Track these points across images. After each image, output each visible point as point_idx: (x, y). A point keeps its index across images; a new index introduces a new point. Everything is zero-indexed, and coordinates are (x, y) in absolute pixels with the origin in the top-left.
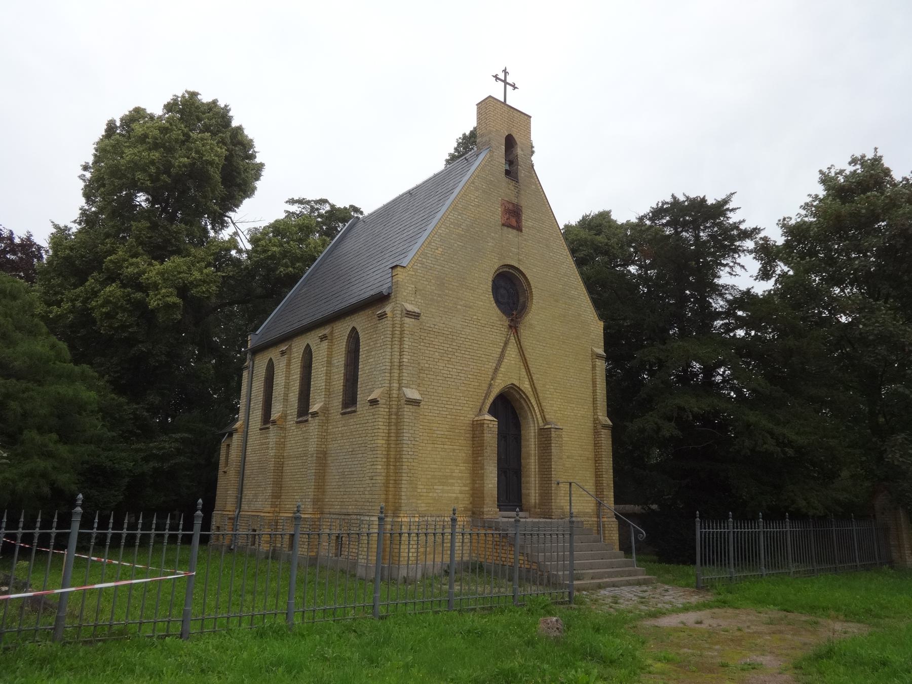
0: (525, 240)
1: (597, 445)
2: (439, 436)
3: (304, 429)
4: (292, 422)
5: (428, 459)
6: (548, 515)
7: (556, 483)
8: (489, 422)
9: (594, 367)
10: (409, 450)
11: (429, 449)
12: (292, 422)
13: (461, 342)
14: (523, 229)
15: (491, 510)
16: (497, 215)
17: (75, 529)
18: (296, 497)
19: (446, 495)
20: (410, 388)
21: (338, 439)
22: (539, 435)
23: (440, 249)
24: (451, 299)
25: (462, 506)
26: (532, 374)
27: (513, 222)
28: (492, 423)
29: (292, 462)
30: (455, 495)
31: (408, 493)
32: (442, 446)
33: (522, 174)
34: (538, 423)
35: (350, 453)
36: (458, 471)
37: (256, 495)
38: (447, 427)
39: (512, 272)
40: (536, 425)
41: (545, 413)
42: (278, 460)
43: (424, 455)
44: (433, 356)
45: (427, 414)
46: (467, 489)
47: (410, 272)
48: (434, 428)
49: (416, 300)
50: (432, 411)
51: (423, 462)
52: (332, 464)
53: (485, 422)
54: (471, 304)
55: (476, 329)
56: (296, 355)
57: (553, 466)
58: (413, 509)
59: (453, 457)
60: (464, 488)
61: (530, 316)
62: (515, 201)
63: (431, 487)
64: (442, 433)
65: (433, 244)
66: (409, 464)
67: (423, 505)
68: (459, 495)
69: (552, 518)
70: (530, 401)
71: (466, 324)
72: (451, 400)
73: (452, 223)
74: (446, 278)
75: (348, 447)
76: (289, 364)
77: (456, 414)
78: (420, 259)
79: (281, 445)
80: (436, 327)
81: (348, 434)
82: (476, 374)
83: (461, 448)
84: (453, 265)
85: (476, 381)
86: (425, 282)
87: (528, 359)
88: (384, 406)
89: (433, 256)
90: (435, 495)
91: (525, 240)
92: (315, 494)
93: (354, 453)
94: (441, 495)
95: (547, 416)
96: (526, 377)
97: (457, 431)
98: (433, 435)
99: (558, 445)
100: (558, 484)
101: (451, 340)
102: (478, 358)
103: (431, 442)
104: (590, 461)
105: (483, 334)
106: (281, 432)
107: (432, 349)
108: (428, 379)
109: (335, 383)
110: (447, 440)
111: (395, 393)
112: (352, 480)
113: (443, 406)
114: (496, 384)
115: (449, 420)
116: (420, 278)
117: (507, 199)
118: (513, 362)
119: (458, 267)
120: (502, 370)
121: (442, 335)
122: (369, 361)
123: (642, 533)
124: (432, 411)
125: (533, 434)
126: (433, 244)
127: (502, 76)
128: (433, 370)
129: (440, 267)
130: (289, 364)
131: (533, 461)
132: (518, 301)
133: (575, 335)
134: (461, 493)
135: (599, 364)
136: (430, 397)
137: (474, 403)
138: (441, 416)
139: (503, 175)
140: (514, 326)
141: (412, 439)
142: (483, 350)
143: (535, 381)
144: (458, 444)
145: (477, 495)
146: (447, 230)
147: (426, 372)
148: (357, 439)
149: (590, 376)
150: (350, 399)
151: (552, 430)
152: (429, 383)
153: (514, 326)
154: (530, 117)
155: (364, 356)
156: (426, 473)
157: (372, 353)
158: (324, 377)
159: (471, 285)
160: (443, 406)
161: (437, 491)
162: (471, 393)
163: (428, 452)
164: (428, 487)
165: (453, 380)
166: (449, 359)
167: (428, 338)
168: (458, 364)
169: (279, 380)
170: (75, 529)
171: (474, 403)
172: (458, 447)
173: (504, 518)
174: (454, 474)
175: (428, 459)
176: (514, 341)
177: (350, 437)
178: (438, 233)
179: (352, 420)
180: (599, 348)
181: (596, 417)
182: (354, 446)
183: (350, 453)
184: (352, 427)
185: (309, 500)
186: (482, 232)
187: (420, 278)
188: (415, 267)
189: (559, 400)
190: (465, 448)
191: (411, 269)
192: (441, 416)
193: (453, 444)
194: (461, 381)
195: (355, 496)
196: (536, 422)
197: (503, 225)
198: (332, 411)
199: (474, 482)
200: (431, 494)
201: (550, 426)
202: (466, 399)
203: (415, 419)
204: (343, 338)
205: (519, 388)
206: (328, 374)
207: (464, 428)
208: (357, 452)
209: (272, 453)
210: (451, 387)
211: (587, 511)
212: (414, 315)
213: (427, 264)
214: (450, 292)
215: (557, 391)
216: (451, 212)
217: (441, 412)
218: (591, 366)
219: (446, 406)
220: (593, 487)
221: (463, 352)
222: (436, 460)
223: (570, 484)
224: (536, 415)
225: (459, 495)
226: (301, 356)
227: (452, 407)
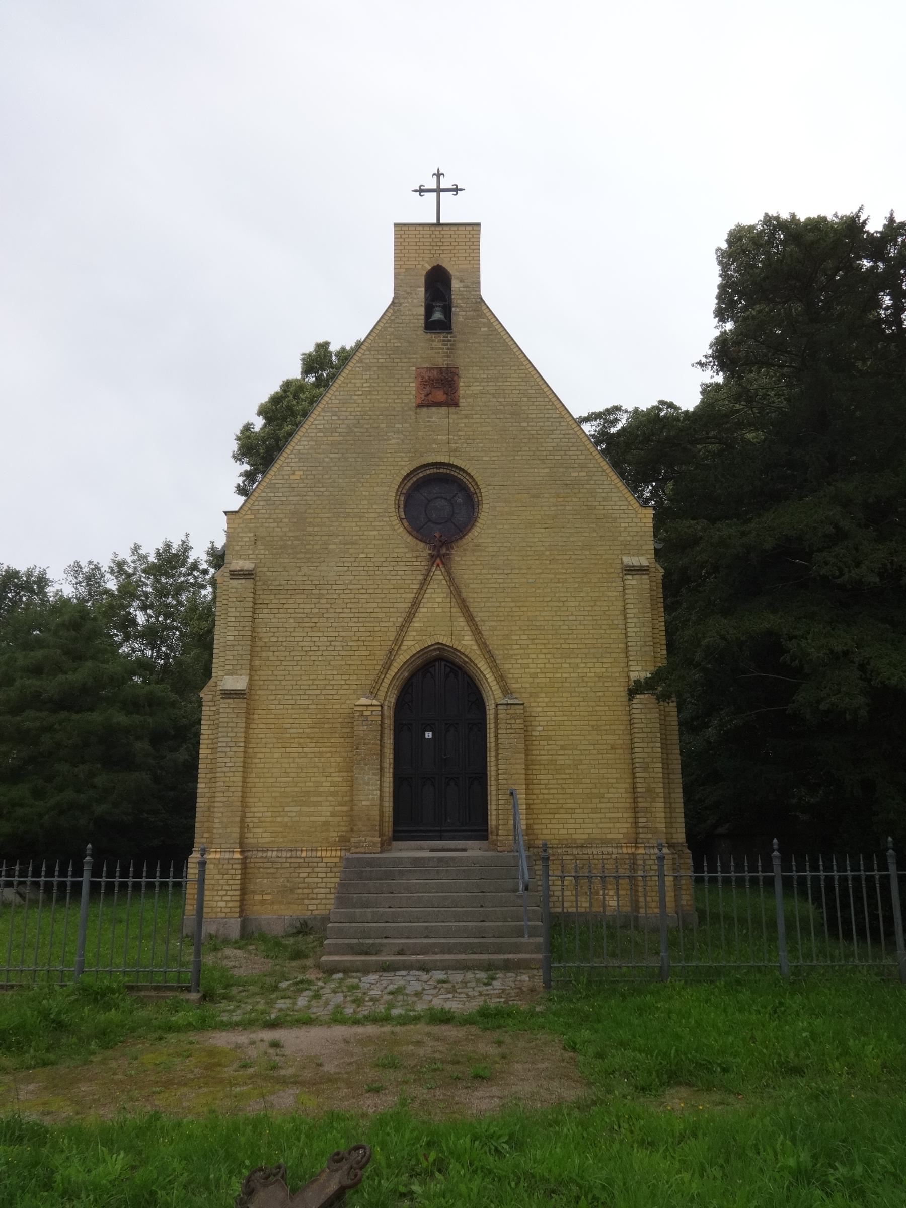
0: (466, 417)
2: (293, 736)
7: (509, 792)
8: (365, 708)
11: (276, 755)
13: (335, 596)
17: (86, 878)
19: (307, 819)
20: (236, 674)
24: (317, 538)
25: (335, 834)
27: (440, 396)
30: (323, 819)
31: (225, 820)
32: (300, 750)
33: (459, 316)
36: (329, 784)
38: (309, 721)
39: (445, 471)
44: (287, 625)
45: (273, 707)
48: (285, 726)
49: (257, 552)
50: (283, 702)
51: (267, 775)
54: (355, 538)
58: (232, 841)
59: (320, 765)
61: (475, 531)
63: (280, 809)
64: (301, 731)
67: (264, 835)
68: (330, 819)
73: (320, 430)
74: (308, 511)
77: (325, 702)
78: (264, 494)
80: (290, 583)
83: (334, 750)
84: (322, 490)
85: (364, 648)
86: (272, 525)
89: (285, 485)
90: (286, 820)
91: (466, 417)
94: (298, 819)
96: (467, 628)
98: (284, 736)
101: (317, 596)
102: (368, 615)
103: (280, 745)
105: (378, 577)
107: (283, 615)
108: (275, 658)
110: (308, 740)
113: (302, 692)
115: (313, 711)
117: (427, 365)
118: (440, 610)
120: (416, 624)
121: (300, 592)
124: (283, 702)
126: (285, 468)
128: (284, 644)
129: (298, 498)
133: (580, 543)
134: (333, 814)
135: (634, 582)
136: (278, 683)
138: (298, 707)
141: (232, 744)
144: (330, 745)
146: (311, 443)
147: (272, 649)
152: (278, 663)
154: (479, 225)
156: (271, 789)
160: (302, 692)
161: (289, 814)
162: (353, 668)
163: (275, 760)
164: (275, 810)
166: (313, 625)
167: (277, 601)
170: (86, 878)
172: (328, 750)
174: (321, 789)
176: (442, 577)
178: (295, 452)
188: (257, 507)
190: (342, 750)
191: (249, 512)
192: (298, 707)
193: (318, 745)
194: (336, 653)
197: (419, 406)
200: (279, 820)
202: (344, 677)
203: (237, 716)
205: (452, 648)
207: (340, 720)
210: (317, 663)
211: (609, 836)
212: (244, 575)
213: (276, 499)
215: (536, 641)
217: (298, 702)
219: (308, 692)
221: (341, 610)
222: (288, 770)
225: (330, 819)
227: (318, 692)
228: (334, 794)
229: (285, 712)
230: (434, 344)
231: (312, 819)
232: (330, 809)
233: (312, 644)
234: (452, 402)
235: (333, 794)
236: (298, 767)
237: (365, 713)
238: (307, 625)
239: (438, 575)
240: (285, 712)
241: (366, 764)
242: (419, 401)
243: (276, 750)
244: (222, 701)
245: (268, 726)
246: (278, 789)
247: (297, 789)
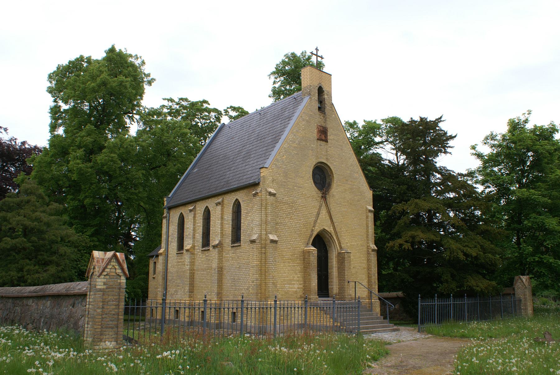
0: (330, 147)
1: (368, 260)
2: (287, 259)
3: (207, 254)
4: (199, 250)
5: (282, 271)
6: (342, 298)
8: (313, 251)
9: (367, 217)
10: (273, 267)
11: (282, 266)
12: (199, 250)
13: (297, 207)
14: (328, 141)
15: (314, 297)
18: (204, 292)
21: (230, 260)
22: (338, 256)
23: (285, 156)
26: (334, 223)
28: (315, 251)
29: (200, 273)
30: (295, 290)
31: (273, 289)
32: (288, 264)
33: (328, 108)
34: (337, 250)
35: (238, 268)
36: (296, 277)
37: (176, 291)
40: (336, 251)
41: (341, 244)
42: (191, 271)
43: (279, 269)
45: (280, 247)
46: (301, 286)
47: (270, 170)
50: (283, 245)
52: (226, 274)
53: (311, 250)
55: (304, 200)
56: (199, 212)
57: (346, 273)
59: (294, 270)
60: (300, 286)
62: (324, 125)
63: (283, 286)
64: (288, 257)
65: (281, 153)
66: (273, 274)
69: (345, 301)
70: (333, 238)
71: (299, 197)
72: (292, 239)
75: (236, 265)
80: (284, 200)
81: (236, 258)
82: (305, 224)
83: (298, 265)
85: (305, 228)
87: (332, 215)
88: (259, 244)
92: (218, 290)
93: (240, 268)
95: (342, 246)
97: (296, 256)
99: (348, 261)
100: (349, 282)
104: (365, 269)
105: (308, 202)
106: (192, 256)
109: (226, 229)
110: (291, 261)
111: (263, 237)
112: (239, 282)
113: (288, 242)
114: (316, 229)
116: (275, 173)
118: (324, 217)
119: (295, 165)
122: (248, 218)
123: (393, 307)
124: (283, 245)
125: (335, 256)
127: (315, 52)
129: (285, 166)
131: (335, 270)
132: (326, 182)
134: (298, 288)
135: (370, 215)
136: (281, 238)
137: (304, 240)
139: (317, 111)
140: (324, 197)
141: (274, 261)
142: (309, 211)
143: (336, 227)
145: (306, 289)
148: (242, 261)
149: (365, 222)
150: (236, 238)
151: (345, 253)
153: (324, 197)
154: (331, 75)
155: (244, 215)
156: (281, 278)
157: (250, 214)
158: (220, 226)
159: (302, 175)
160: (288, 242)
162: (302, 235)
163: (281, 267)
165: (293, 228)
166: (291, 217)
168: (295, 219)
169: (189, 225)
171: (304, 240)
173: (321, 301)
174: (295, 279)
175: (282, 271)
177: (237, 260)
179: (238, 251)
180: (370, 206)
181: (368, 245)
182: (240, 265)
183: (238, 268)
184: (238, 254)
185: (214, 293)
186: (306, 144)
187: (275, 173)
188: (273, 167)
189: (348, 236)
193: (294, 263)
195: (242, 291)
196: (336, 249)
197: (318, 139)
198: (225, 245)
199: (305, 282)
201: (344, 252)
204: (230, 204)
207: (299, 254)
208: (242, 268)
209: (188, 267)
211: (363, 296)
214: (291, 180)
216: (290, 135)
218: (366, 217)
219: (290, 242)
220: (366, 283)
222: (285, 271)
223: (355, 282)
224: (336, 245)
225: (298, 290)
226: (203, 213)
227: (293, 243)
228: (298, 281)
229: (283, 249)
230: (321, 117)
231: (293, 290)
232: (297, 286)
233: (291, 224)
235: (298, 281)
236: (288, 270)
237: (314, 252)
238: (289, 217)
240: (283, 249)
241: (314, 271)
242: (318, 138)
243: (282, 264)
244: (270, 244)
245: (279, 254)
246: (282, 278)
247: (288, 279)
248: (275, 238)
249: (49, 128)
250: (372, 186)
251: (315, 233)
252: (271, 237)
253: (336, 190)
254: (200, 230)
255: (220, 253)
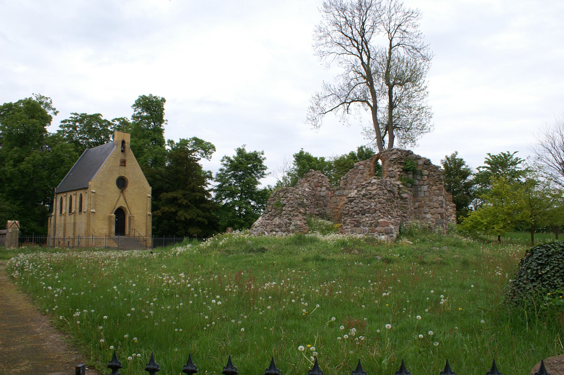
1: (147, 220)
15: (113, 235)
16: (119, 163)
37: (59, 233)
76: (66, 199)
79: (65, 220)
130: (66, 199)
140: (122, 192)
145: (110, 232)
149: (146, 202)
150: (80, 210)
153: (122, 192)
169: (64, 203)
197: (120, 166)
206: (76, 204)
209: (63, 222)
234: (125, 166)
239: (122, 195)
248: (94, 211)
249: (2, 105)
250: (151, 186)
251: (116, 208)
252: (92, 211)
253: (129, 189)
254: (68, 205)
255: (75, 216)
